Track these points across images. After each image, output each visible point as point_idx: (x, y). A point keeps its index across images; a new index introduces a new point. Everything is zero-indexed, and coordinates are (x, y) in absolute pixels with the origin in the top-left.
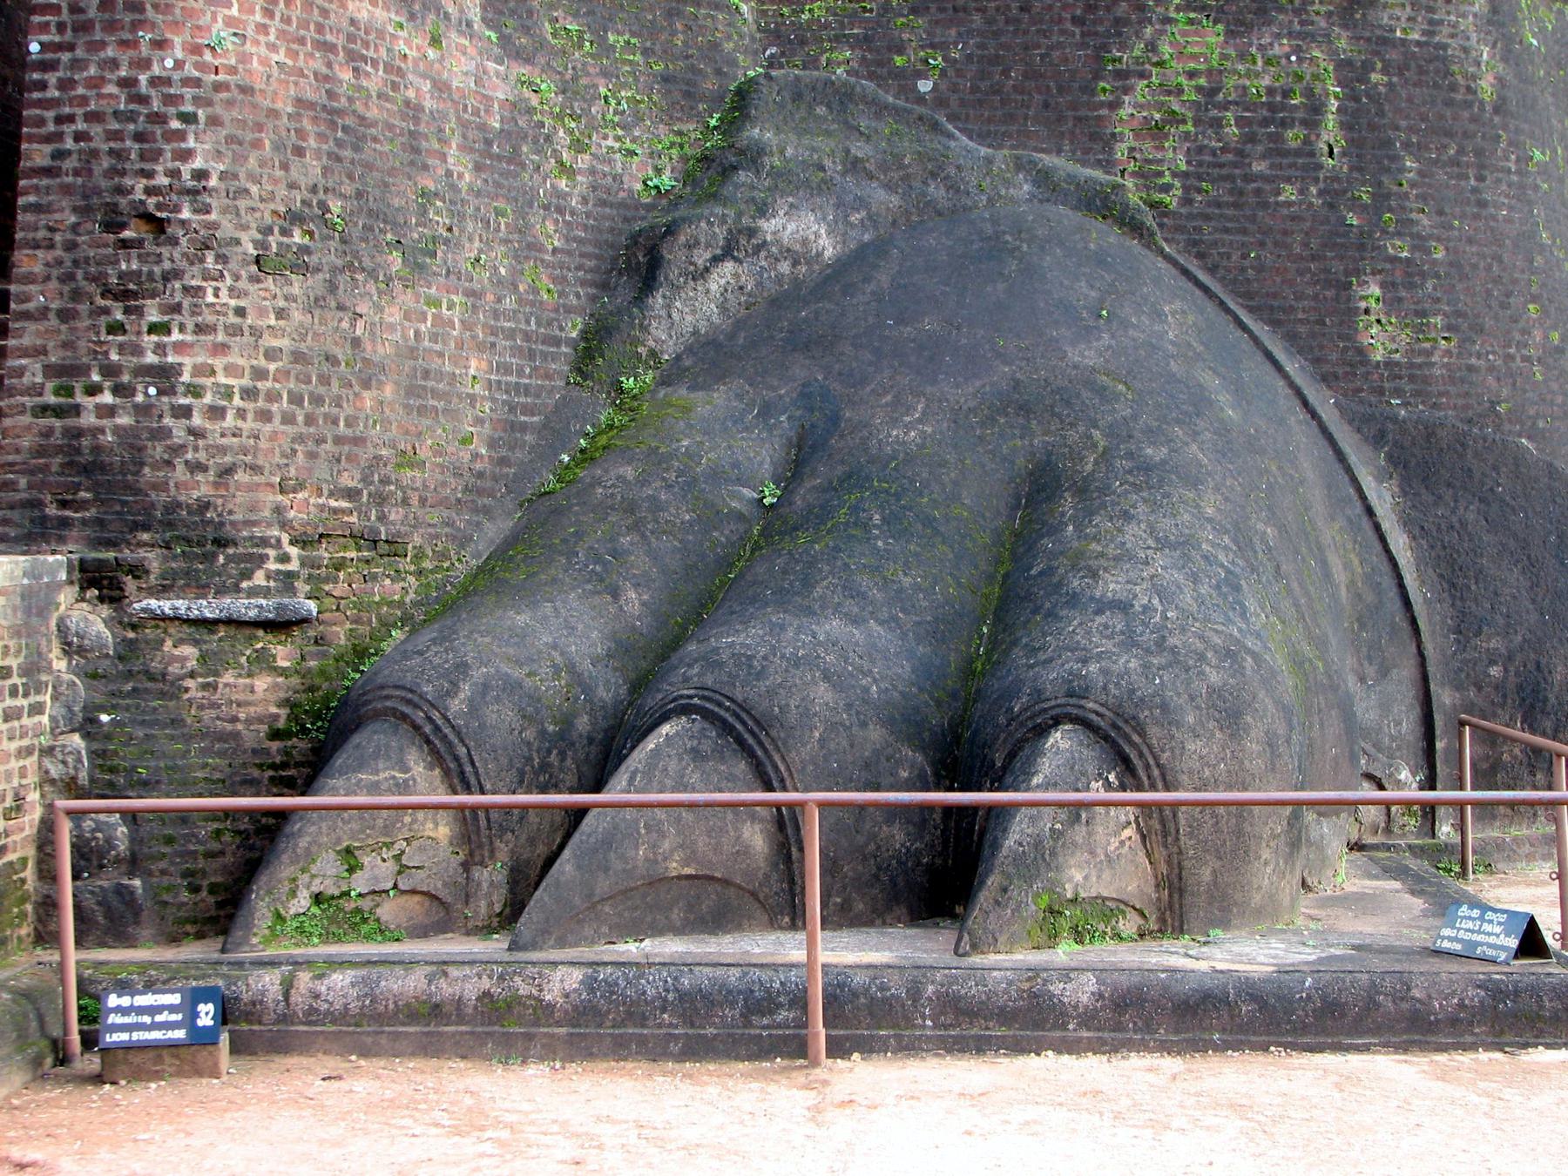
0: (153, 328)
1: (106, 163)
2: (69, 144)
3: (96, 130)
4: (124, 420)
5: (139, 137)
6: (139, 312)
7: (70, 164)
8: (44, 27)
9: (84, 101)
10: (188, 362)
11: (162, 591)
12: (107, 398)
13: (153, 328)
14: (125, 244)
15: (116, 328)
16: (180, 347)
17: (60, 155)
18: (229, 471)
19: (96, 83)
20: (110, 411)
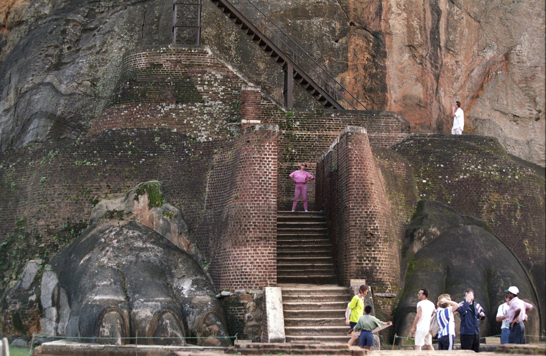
0: (374, 251)
1: (364, 225)
2: (358, 222)
3: (362, 219)
4: (370, 265)
5: (369, 221)
6: (371, 248)
7: (358, 224)
8: (352, 203)
9: (359, 215)
10: (378, 256)
11: (377, 292)
12: (367, 262)
13: (374, 251)
14: (368, 238)
15: (368, 251)
16: (377, 254)
17: (356, 223)
18: (384, 273)
19: (361, 212)
20: (367, 264)
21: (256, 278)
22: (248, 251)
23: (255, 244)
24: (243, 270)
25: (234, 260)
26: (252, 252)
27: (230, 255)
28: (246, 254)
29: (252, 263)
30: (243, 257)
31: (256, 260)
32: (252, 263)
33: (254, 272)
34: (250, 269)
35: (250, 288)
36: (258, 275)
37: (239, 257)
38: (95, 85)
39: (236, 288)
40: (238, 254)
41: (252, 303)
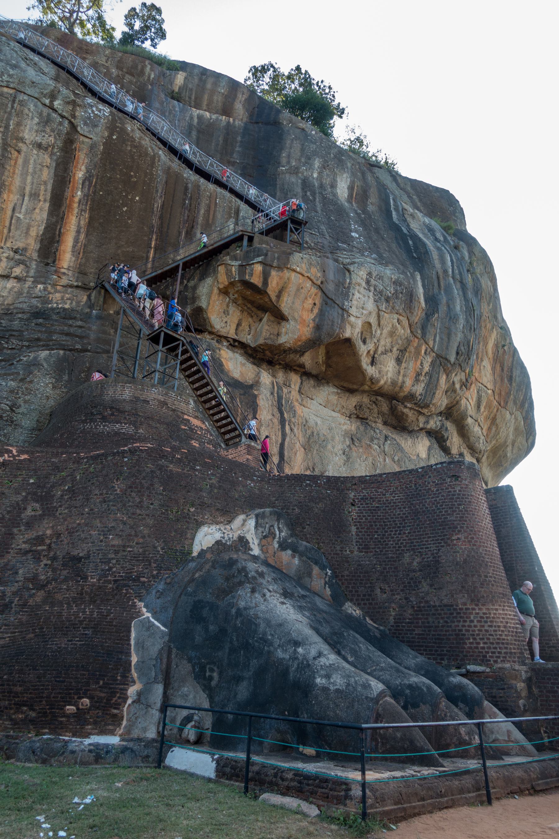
21: (514, 649)
22: (497, 610)
23: (501, 602)
24: (498, 637)
25: (478, 621)
26: (501, 612)
27: (472, 613)
28: (495, 614)
29: (505, 627)
30: (493, 618)
31: (507, 623)
32: (505, 627)
33: (511, 640)
34: (506, 635)
35: (514, 662)
36: (515, 644)
37: (487, 617)
38: (14, 411)
39: (496, 662)
40: (484, 614)
41: (523, 685)
